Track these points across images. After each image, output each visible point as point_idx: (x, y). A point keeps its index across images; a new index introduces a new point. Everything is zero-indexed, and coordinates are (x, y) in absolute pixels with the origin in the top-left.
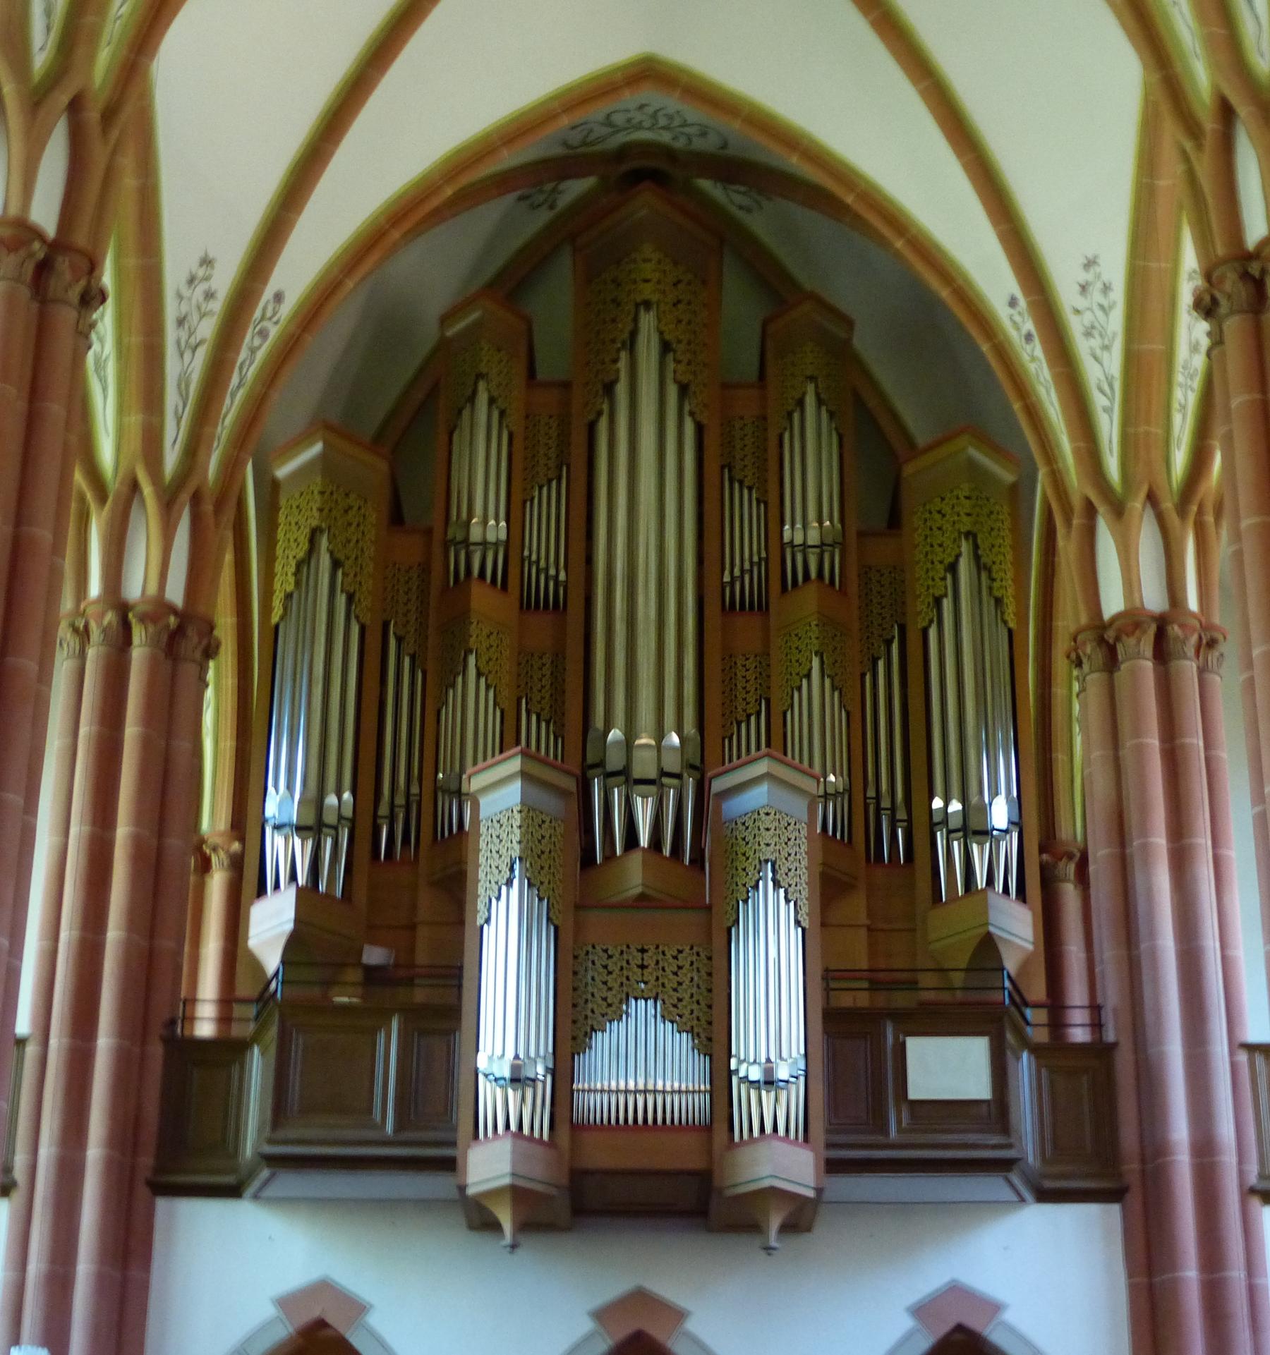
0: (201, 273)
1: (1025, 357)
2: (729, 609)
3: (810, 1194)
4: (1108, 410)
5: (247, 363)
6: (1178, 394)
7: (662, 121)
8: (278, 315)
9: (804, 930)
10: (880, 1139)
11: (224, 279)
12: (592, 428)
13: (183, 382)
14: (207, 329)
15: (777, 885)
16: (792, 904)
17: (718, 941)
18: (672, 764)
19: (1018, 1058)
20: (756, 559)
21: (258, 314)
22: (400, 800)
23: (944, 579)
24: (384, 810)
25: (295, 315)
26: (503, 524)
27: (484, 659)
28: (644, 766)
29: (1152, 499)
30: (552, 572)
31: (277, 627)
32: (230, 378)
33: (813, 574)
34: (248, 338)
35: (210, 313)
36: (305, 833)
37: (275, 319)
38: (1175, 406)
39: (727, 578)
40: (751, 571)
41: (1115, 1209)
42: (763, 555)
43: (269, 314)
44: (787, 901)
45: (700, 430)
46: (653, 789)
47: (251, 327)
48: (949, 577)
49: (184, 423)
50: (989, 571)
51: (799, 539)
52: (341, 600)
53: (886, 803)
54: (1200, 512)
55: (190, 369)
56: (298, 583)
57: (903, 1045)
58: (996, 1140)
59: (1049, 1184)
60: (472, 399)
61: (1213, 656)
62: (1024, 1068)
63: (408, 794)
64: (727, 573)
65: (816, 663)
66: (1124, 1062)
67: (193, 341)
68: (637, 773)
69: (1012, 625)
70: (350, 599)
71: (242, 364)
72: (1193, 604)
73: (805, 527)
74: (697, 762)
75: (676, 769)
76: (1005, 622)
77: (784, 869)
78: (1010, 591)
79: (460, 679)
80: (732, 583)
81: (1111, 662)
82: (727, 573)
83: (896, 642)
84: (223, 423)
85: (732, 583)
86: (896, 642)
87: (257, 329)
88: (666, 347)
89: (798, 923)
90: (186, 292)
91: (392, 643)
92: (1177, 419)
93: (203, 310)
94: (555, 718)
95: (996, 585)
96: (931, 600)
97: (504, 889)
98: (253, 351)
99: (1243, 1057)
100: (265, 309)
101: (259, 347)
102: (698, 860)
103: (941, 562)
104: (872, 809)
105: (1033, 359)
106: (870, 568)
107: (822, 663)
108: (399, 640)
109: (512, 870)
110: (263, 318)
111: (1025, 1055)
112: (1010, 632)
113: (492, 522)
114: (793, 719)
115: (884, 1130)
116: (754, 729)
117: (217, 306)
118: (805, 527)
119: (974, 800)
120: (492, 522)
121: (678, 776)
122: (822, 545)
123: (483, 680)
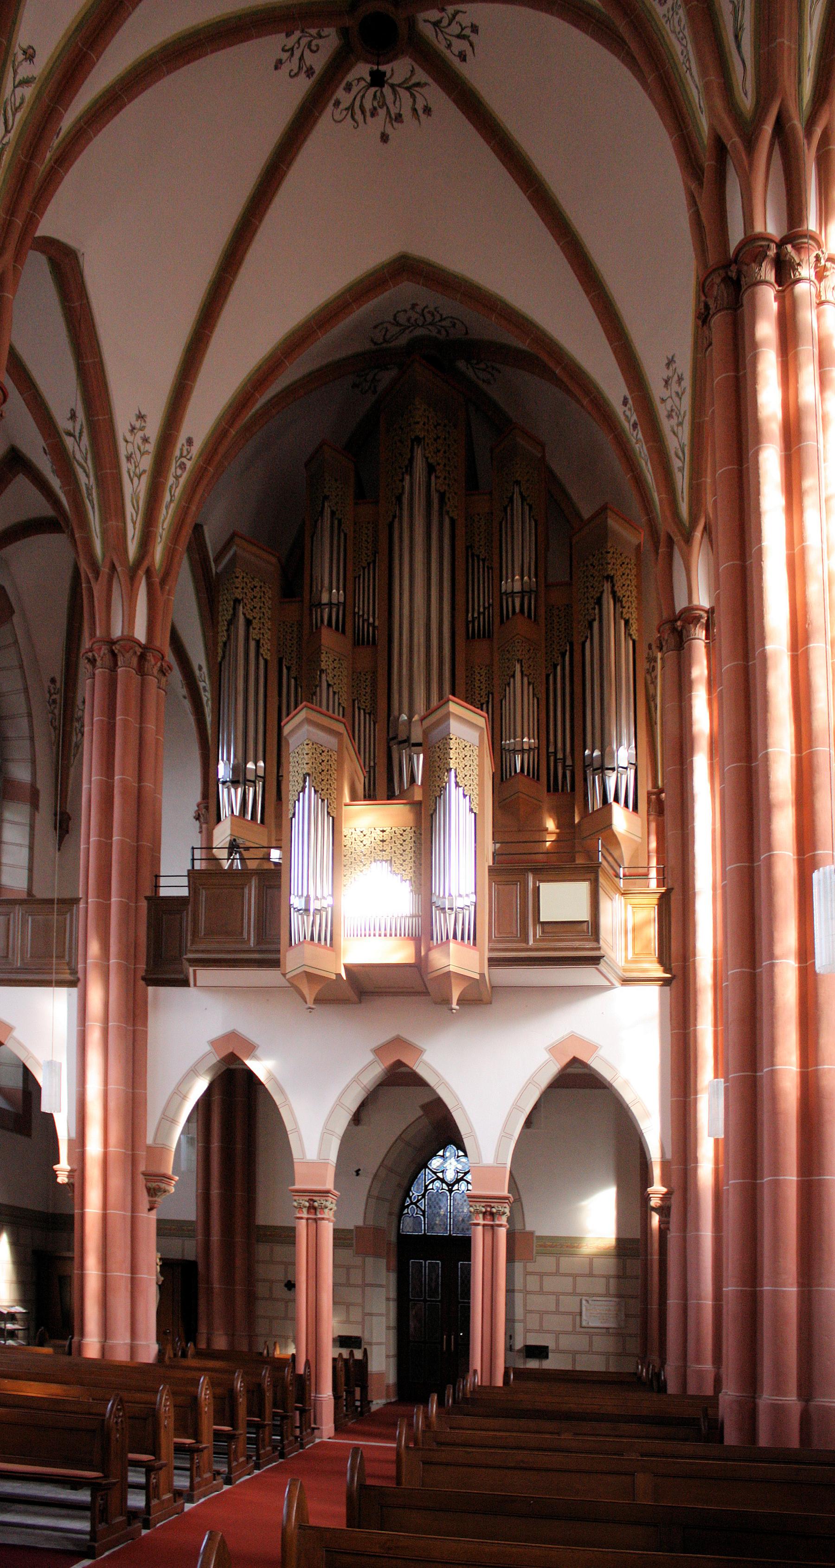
3: (477, 977)
5: (174, 486)
8: (190, 455)
9: (475, 814)
10: (523, 945)
12: (391, 526)
13: (135, 496)
15: (457, 785)
20: (486, 605)
21: (177, 453)
23: (594, 609)
25: (200, 455)
32: (162, 496)
33: (517, 609)
34: (173, 469)
35: (147, 452)
37: (188, 457)
39: (470, 619)
40: (484, 613)
43: (185, 453)
47: (174, 462)
48: (597, 607)
49: (138, 526)
50: (621, 602)
51: (509, 591)
55: (139, 490)
57: (539, 887)
60: (322, 512)
64: (470, 615)
69: (634, 637)
71: (171, 487)
76: (630, 635)
78: (635, 615)
80: (473, 621)
82: (470, 615)
83: (568, 653)
84: (162, 526)
86: (568, 653)
87: (178, 463)
89: (471, 810)
90: (130, 438)
93: (142, 451)
95: (625, 611)
96: (586, 623)
98: (177, 477)
100: (182, 450)
101: (181, 476)
103: (592, 598)
106: (553, 606)
107: (522, 666)
110: (181, 456)
112: (634, 642)
115: (526, 941)
122: (522, 592)
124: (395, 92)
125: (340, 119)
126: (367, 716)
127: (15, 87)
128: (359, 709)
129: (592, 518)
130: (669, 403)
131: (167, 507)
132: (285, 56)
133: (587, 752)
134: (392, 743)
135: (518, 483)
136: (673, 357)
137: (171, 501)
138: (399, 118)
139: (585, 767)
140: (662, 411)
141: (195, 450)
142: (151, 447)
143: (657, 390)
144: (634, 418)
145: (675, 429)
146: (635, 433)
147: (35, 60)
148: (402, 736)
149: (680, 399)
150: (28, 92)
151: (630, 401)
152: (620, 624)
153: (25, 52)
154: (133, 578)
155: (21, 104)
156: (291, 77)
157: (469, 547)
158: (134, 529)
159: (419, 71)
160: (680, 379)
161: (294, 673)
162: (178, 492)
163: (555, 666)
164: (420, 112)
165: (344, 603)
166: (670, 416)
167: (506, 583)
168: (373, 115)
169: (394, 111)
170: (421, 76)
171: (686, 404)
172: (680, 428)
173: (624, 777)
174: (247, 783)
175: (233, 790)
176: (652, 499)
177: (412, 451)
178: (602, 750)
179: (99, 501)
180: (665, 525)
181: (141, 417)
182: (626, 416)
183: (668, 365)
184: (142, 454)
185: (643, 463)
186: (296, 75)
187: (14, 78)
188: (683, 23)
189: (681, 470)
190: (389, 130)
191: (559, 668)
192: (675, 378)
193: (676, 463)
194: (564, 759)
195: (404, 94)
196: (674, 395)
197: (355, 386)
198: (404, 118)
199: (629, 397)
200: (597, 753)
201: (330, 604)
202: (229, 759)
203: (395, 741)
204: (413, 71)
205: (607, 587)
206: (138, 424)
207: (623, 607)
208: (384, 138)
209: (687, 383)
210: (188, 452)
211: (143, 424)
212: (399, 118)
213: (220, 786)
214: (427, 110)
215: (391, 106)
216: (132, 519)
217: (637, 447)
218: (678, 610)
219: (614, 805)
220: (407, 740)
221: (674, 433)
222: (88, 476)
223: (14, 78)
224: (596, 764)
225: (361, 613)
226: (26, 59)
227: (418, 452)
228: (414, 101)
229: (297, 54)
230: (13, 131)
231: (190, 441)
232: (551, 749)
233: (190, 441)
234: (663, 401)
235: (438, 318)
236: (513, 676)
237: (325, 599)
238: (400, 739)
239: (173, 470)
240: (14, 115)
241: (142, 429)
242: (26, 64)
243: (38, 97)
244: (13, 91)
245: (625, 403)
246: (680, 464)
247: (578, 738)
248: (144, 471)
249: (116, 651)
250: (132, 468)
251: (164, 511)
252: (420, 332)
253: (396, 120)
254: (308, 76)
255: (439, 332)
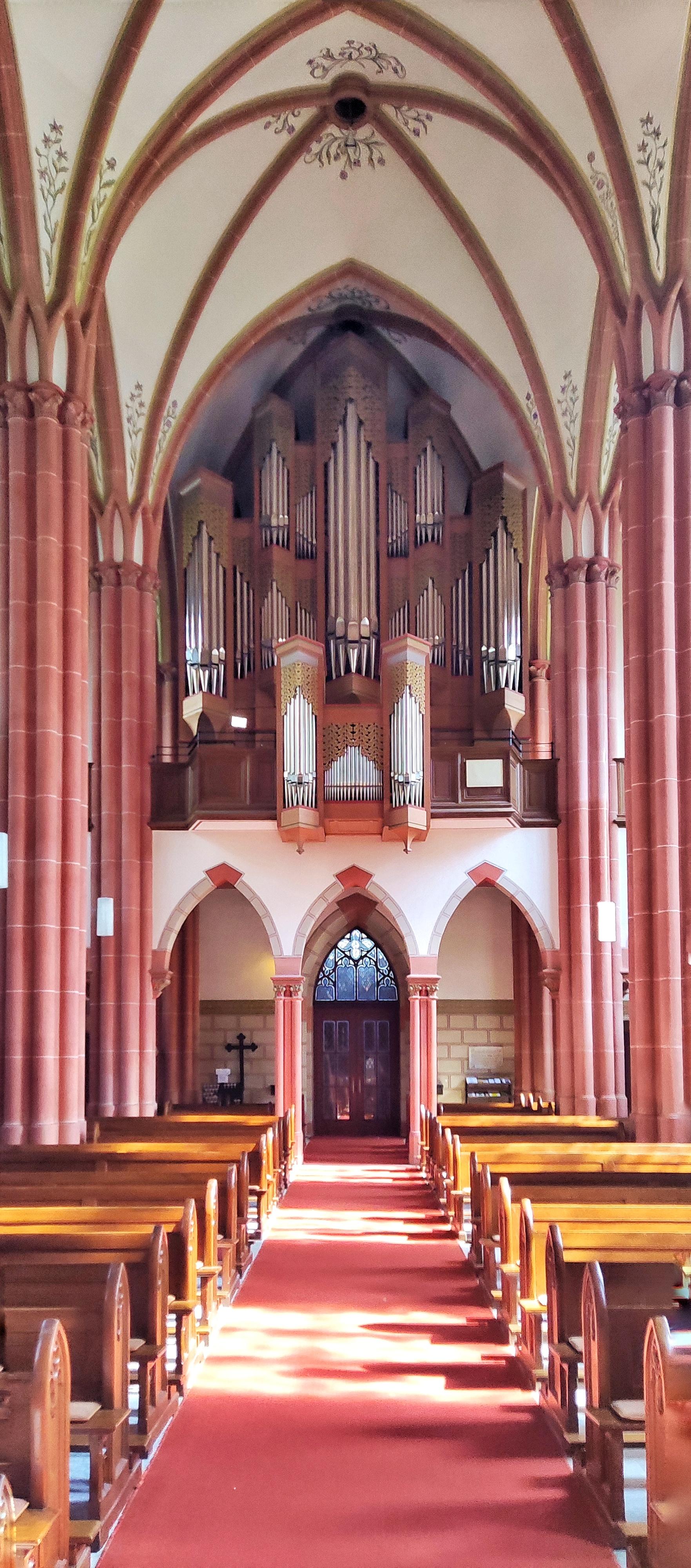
0: (136, 393)
1: (533, 427)
2: (391, 555)
4: (572, 455)
6: (606, 446)
7: (357, 294)
11: (148, 396)
12: (326, 466)
14: (142, 423)
16: (418, 704)
17: (386, 722)
18: (365, 632)
19: (515, 767)
21: (165, 414)
22: (245, 651)
24: (238, 656)
26: (286, 517)
27: (280, 584)
28: (353, 635)
29: (590, 501)
30: (310, 540)
31: (185, 570)
34: (162, 426)
36: (204, 668)
38: (604, 452)
39: (390, 541)
41: (555, 829)
42: (407, 529)
44: (416, 702)
45: (377, 465)
46: (357, 645)
52: (214, 556)
53: (461, 648)
54: (612, 506)
56: (194, 549)
58: (505, 803)
59: (526, 820)
60: (270, 452)
61: (614, 578)
62: (517, 771)
63: (249, 647)
65: (430, 582)
66: (561, 766)
67: (135, 430)
68: (350, 639)
69: (521, 562)
70: (218, 555)
72: (605, 553)
73: (426, 514)
74: (376, 631)
75: (367, 635)
76: (518, 561)
77: (415, 688)
78: (521, 545)
79: (269, 594)
80: (392, 544)
81: (567, 582)
85: (392, 544)
88: (360, 423)
90: (130, 403)
91: (238, 575)
92: (604, 458)
94: (312, 611)
97: (292, 699)
99: (614, 764)
100: (168, 412)
102: (377, 677)
104: (454, 652)
105: (537, 427)
108: (241, 574)
109: (296, 691)
110: (168, 416)
111: (518, 765)
112: (520, 565)
113: (281, 516)
114: (420, 608)
116: (401, 617)
117: (145, 410)
118: (426, 514)
119: (501, 647)
120: (281, 516)
121: (368, 638)
123: (280, 594)
125: (310, 161)
126: (308, 615)
127: (100, 188)
128: (301, 609)
129: (490, 470)
130: (564, 405)
133: (484, 648)
134: (329, 637)
135: (430, 438)
136: (570, 372)
139: (482, 659)
140: (558, 410)
143: (555, 393)
144: (535, 410)
145: (569, 423)
146: (535, 422)
147: (115, 168)
148: (340, 632)
149: (574, 404)
150: (109, 192)
151: (532, 397)
152: (510, 552)
153: (108, 163)
154: (133, 514)
155: (104, 199)
156: (276, 132)
157: (389, 484)
160: (574, 389)
161: (246, 578)
163: (457, 581)
165: (289, 525)
166: (564, 414)
167: (421, 514)
168: (336, 158)
171: (578, 407)
172: (572, 424)
173: (513, 667)
174: (214, 666)
175: (201, 671)
176: (547, 471)
177: (346, 409)
178: (496, 647)
179: (102, 451)
180: (557, 496)
181: (139, 387)
182: (528, 408)
183: (565, 377)
184: (138, 416)
185: (541, 447)
186: (281, 131)
187: (101, 181)
188: (614, 207)
189: (572, 455)
191: (460, 581)
192: (571, 388)
193: (567, 450)
194: (464, 651)
196: (568, 400)
198: (362, 165)
199: (531, 393)
200: (492, 650)
201: (278, 527)
202: (197, 648)
203: (333, 636)
205: (500, 524)
207: (513, 540)
209: (580, 392)
213: (188, 666)
217: (536, 432)
218: (565, 560)
219: (506, 690)
220: (345, 637)
221: (567, 427)
223: (101, 181)
224: (491, 657)
225: (301, 533)
226: (109, 168)
227: (351, 408)
228: (372, 153)
230: (97, 222)
232: (454, 643)
233: (175, 404)
234: (559, 402)
235: (364, 295)
236: (427, 589)
237: (274, 522)
238: (338, 635)
240: (99, 209)
242: (109, 171)
243: (116, 194)
244: (99, 192)
245: (528, 397)
246: (571, 451)
247: (476, 635)
249: (121, 573)
252: (348, 302)
254: (289, 133)
255: (364, 303)
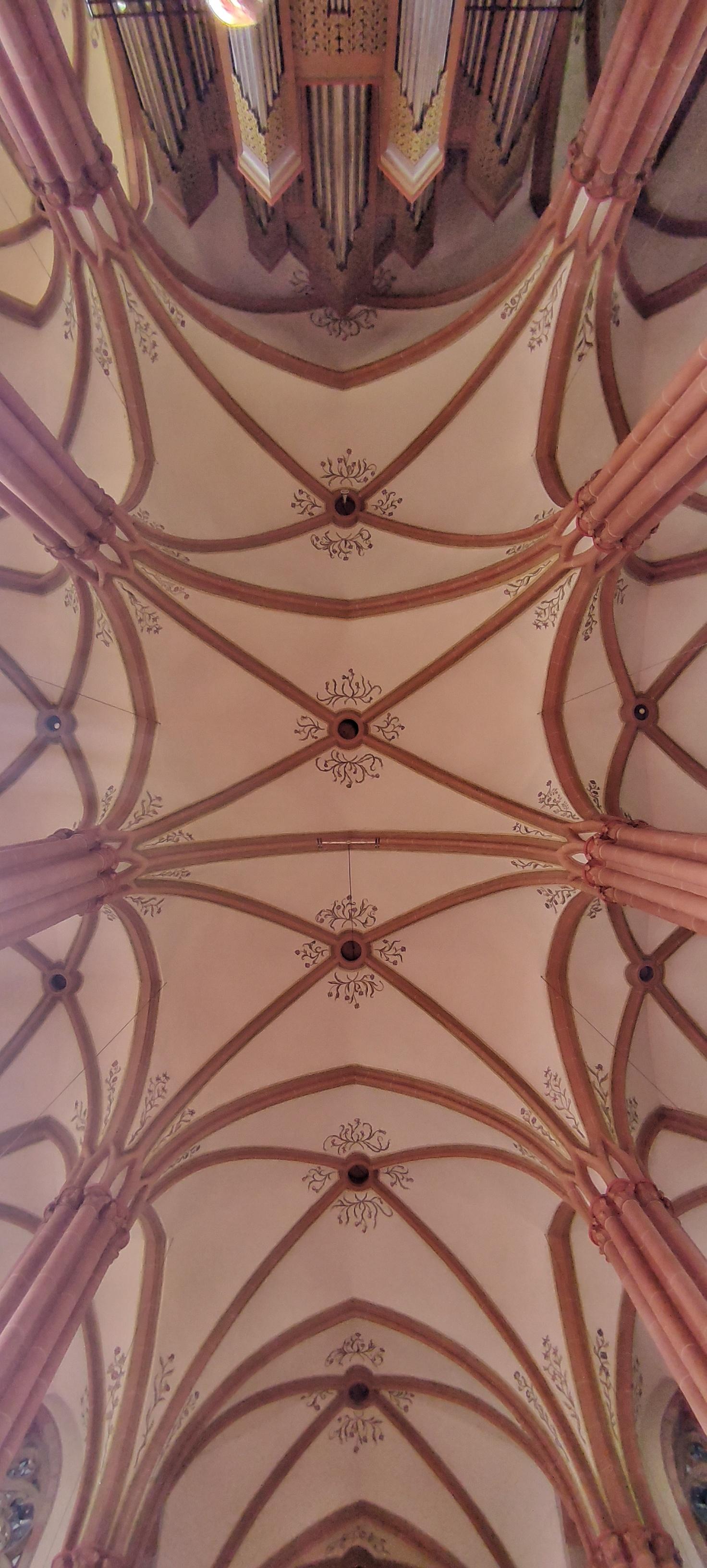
21: (514, 312)
43: (509, 310)
98: (519, 296)
100: (511, 312)
110: (512, 309)
124: (341, 473)
131: (533, 278)
132: (396, 503)
137: (529, 281)
138: (340, 461)
141: (501, 309)
142: (531, 325)
158: (562, 275)
159: (326, 485)
162: (522, 286)
164: (327, 463)
169: (343, 464)
170: (325, 482)
190: (346, 455)
195: (336, 472)
197: (394, 278)
204: (330, 483)
206: (535, 343)
208: (349, 451)
210: (506, 309)
211: (532, 341)
212: (340, 461)
214: (323, 464)
215: (344, 467)
216: (561, 283)
222: (586, 316)
229: (389, 502)
231: (503, 316)
233: (503, 316)
239: (521, 303)
241: (533, 339)
248: (541, 311)
250: (549, 317)
251: (536, 277)
253: (341, 459)
